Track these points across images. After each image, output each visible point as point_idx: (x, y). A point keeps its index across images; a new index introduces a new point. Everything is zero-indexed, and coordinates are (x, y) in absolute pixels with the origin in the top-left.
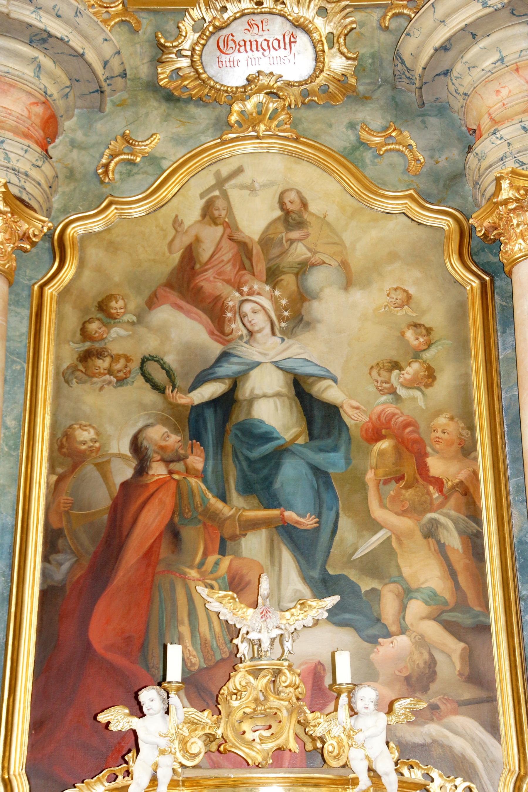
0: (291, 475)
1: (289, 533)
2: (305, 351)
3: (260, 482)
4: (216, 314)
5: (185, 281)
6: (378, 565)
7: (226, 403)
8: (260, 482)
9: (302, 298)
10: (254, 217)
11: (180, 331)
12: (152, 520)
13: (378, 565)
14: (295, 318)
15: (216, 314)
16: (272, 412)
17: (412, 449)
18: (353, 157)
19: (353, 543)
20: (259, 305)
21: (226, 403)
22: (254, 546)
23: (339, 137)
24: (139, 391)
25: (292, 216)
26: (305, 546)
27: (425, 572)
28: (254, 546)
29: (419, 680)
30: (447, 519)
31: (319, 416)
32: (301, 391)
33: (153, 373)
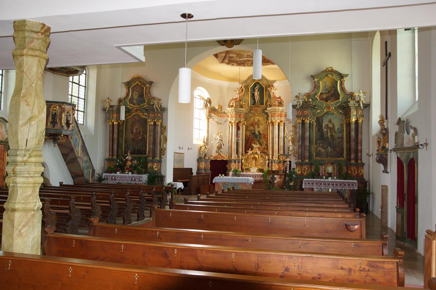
0: (258, 137)
1: (258, 140)
2: (259, 129)
3: (256, 137)
4: (254, 127)
5: (252, 125)
6: (263, 142)
7: (254, 132)
8: (256, 137)
9: (259, 126)
10: (256, 121)
11: (252, 128)
12: (250, 139)
13: (263, 142)
14: (258, 127)
15: (254, 127)
16: (257, 133)
17: (265, 135)
18: (262, 116)
19: (261, 141)
20: (256, 126)
21: (254, 132)
22: (256, 141)
23: (261, 115)
24: (249, 132)
25: (258, 121)
26: (259, 141)
27: (265, 143)
28: (256, 141)
29: (264, 148)
30: (266, 140)
31: (260, 133)
32: (259, 132)
33: (250, 131)
